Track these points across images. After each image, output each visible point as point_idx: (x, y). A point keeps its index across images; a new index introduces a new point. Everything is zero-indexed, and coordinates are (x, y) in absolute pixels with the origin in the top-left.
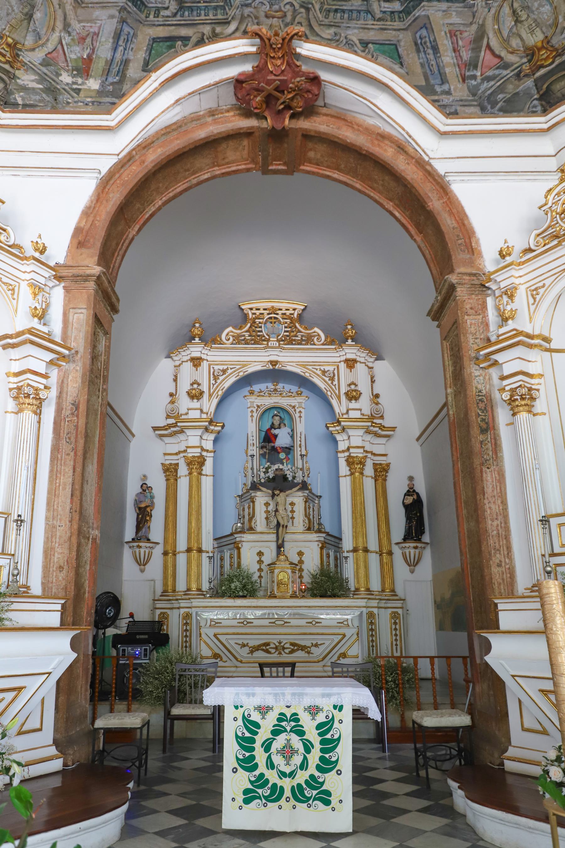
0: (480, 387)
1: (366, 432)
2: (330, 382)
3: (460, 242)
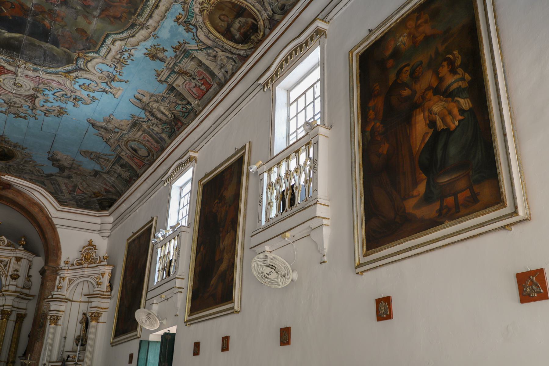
0: (44, 310)
1: (17, 297)
2: (3, 267)
3: (54, 252)
